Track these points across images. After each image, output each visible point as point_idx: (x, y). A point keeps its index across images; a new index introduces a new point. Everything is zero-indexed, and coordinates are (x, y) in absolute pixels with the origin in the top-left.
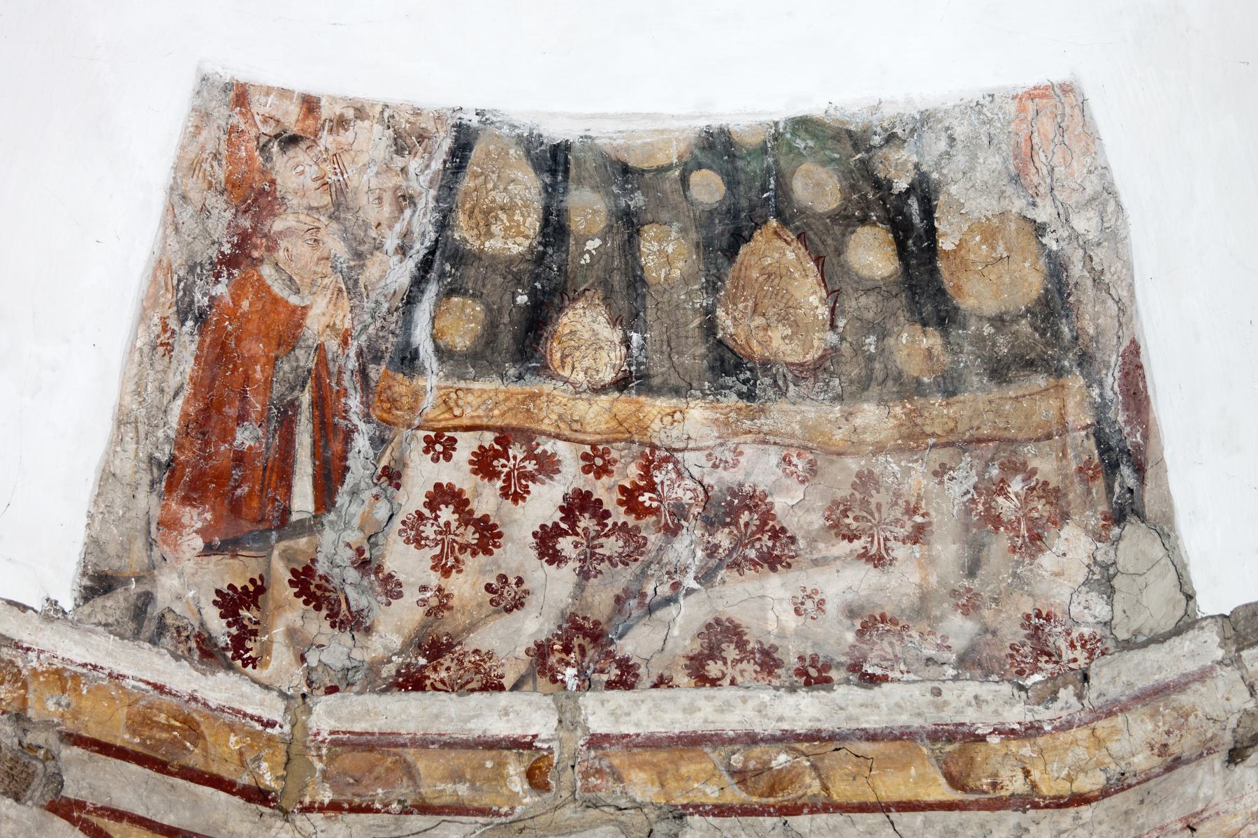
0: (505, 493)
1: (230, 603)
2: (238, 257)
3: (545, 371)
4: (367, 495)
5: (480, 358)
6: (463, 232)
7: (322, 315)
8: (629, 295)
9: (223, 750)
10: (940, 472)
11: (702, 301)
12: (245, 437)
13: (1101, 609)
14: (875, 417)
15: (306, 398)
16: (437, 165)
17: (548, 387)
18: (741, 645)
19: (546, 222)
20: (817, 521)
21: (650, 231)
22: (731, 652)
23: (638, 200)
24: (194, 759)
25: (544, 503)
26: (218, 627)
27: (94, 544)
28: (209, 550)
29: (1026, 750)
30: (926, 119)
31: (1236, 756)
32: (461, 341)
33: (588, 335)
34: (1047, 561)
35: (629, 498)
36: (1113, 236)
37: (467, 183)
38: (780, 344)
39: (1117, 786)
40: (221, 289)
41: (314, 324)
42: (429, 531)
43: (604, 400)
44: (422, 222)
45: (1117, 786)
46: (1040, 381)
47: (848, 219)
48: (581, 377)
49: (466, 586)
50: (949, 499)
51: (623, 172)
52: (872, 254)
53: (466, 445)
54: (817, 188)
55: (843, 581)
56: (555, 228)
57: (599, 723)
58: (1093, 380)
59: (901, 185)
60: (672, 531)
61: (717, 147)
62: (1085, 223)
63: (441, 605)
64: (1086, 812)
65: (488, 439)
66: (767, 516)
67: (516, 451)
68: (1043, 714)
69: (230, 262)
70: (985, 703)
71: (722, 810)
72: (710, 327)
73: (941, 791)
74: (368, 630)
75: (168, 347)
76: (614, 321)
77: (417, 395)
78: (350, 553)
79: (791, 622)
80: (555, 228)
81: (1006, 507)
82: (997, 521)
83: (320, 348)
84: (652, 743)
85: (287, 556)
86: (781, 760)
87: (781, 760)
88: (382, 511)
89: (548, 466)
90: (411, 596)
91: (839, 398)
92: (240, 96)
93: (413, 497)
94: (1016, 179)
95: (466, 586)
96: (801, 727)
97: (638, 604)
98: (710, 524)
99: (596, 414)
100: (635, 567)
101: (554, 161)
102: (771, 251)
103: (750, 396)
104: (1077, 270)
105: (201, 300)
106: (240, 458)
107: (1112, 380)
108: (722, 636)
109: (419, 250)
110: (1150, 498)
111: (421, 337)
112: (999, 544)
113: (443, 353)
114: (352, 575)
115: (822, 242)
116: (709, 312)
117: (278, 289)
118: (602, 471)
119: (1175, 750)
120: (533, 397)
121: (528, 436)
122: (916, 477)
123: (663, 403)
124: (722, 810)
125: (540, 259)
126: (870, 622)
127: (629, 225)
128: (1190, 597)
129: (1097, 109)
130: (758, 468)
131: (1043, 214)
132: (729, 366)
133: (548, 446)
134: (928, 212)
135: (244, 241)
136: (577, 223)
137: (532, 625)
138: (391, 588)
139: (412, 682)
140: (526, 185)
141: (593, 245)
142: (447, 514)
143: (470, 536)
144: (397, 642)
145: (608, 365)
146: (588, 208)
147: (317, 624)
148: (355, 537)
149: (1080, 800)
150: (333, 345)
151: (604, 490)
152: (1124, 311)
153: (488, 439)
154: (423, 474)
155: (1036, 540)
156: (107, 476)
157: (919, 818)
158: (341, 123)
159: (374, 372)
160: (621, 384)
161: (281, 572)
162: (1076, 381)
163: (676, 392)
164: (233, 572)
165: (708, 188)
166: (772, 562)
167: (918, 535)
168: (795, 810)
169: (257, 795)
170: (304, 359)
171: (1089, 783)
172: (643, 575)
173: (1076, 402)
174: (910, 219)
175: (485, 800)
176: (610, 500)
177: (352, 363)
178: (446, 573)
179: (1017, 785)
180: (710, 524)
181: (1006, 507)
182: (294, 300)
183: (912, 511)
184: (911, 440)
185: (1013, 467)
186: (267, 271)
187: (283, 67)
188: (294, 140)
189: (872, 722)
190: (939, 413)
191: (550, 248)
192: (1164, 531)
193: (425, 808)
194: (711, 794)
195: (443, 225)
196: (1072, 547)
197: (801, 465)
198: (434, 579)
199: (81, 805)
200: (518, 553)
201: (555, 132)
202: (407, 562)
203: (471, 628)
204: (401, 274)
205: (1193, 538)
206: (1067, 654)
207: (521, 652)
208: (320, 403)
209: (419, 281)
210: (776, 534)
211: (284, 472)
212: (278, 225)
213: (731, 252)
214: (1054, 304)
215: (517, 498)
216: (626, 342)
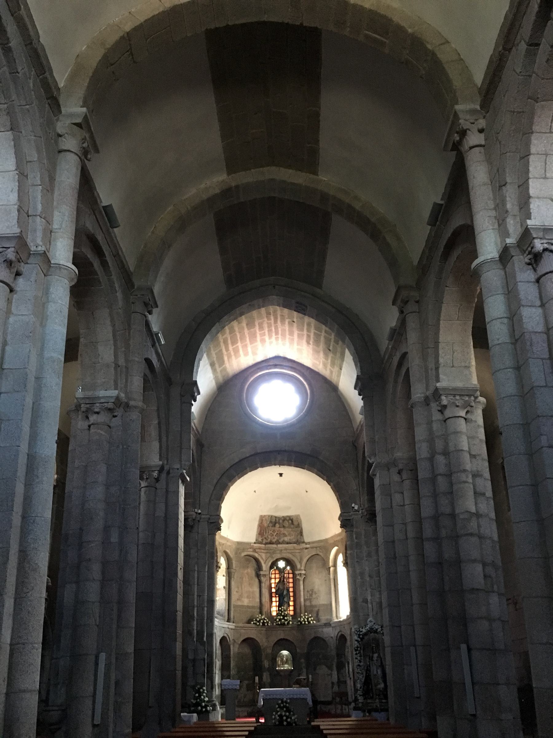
2: (262, 523)
5: (272, 526)
7: (266, 525)
8: (279, 523)
14: (290, 529)
25: (275, 534)
33: (277, 525)
36: (301, 521)
38: (286, 526)
51: (279, 518)
52: (290, 522)
54: (288, 519)
55: (289, 538)
61: (283, 517)
70: (295, 545)
97: (280, 539)
101: (276, 517)
102: (286, 521)
108: (284, 540)
115: (288, 521)
122: (292, 532)
130: (285, 532)
132: (284, 527)
146: (277, 519)
154: (270, 532)
173: (299, 529)
174: (292, 521)
187: (264, 514)
200: (274, 536)
202: (269, 537)
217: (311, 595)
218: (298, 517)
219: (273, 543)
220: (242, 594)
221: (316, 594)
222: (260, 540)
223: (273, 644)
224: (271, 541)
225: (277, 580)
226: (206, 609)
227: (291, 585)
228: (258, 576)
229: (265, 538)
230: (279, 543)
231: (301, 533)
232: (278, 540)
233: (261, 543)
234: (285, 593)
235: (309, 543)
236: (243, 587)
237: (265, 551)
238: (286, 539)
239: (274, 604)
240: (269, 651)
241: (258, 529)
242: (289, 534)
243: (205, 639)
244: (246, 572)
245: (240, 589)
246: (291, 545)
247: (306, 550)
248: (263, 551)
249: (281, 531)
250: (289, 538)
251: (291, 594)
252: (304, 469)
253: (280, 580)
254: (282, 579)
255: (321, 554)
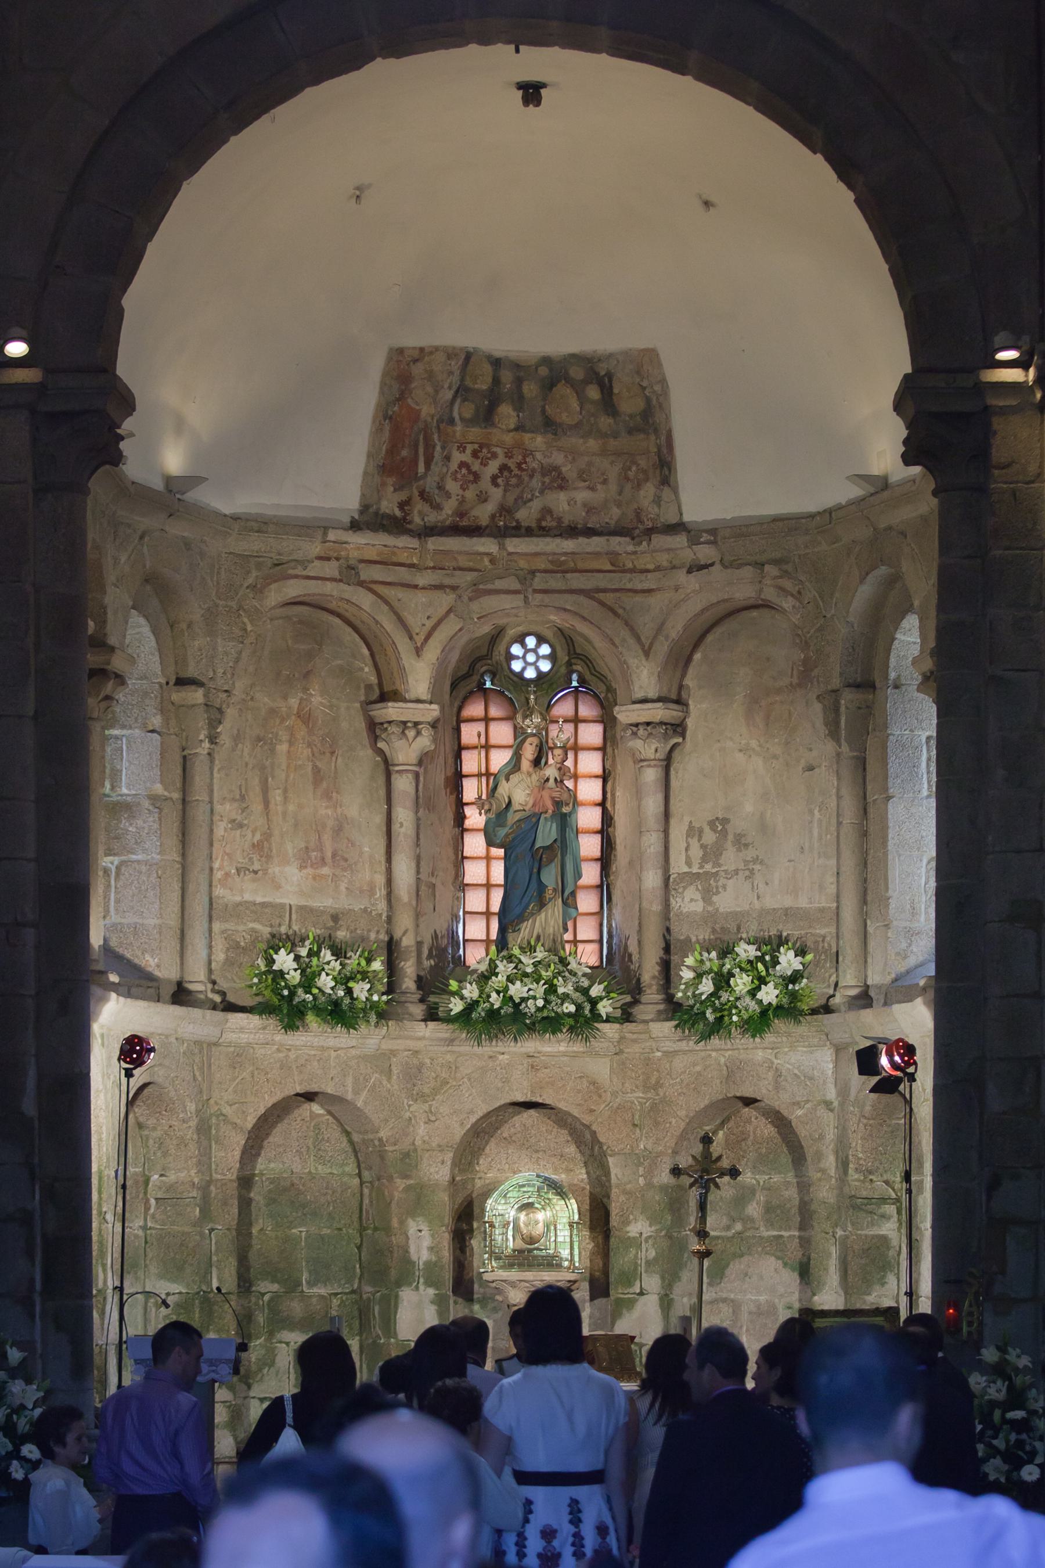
0: (481, 464)
1: (402, 505)
2: (401, 398)
3: (493, 425)
4: (440, 464)
6: (468, 382)
7: (427, 410)
8: (519, 401)
9: (403, 557)
10: (612, 463)
11: (541, 403)
12: (404, 453)
13: (656, 510)
14: (592, 444)
15: (421, 437)
16: (460, 363)
17: (495, 430)
18: (552, 516)
19: (493, 379)
20: (575, 475)
21: (525, 383)
22: (549, 518)
23: (522, 374)
24: (395, 559)
25: (493, 467)
26: (398, 513)
27: (363, 495)
28: (395, 490)
29: (633, 557)
30: (611, 355)
31: (689, 572)
32: (468, 415)
33: (507, 413)
34: (642, 493)
35: (519, 465)
36: (665, 392)
37: (470, 367)
38: (565, 418)
39: (658, 569)
40: (396, 409)
41: (423, 414)
42: (459, 476)
43: (511, 434)
44: (455, 379)
45: (658, 569)
46: (642, 436)
47: (586, 382)
48: (504, 427)
49: (470, 494)
50: (613, 473)
52: (593, 393)
53: (470, 448)
54: (577, 373)
55: (582, 496)
56: (496, 381)
57: (511, 549)
58: (658, 437)
59: (603, 373)
60: (531, 477)
61: (546, 361)
62: (657, 388)
63: (462, 501)
64: (649, 575)
65: (476, 446)
66: (560, 473)
67: (485, 450)
68: (638, 549)
69: (398, 400)
71: (546, 571)
72: (544, 411)
73: (609, 567)
74: (442, 509)
75: (381, 430)
76: (515, 410)
77: (454, 432)
78: (435, 484)
79: (566, 507)
80: (496, 381)
81: (631, 474)
82: (627, 479)
83: (425, 421)
84: (526, 554)
85: (417, 488)
86: (563, 558)
87: (563, 558)
88: (445, 470)
89: (494, 456)
90: (454, 498)
91: (582, 437)
92: (401, 351)
93: (454, 466)
94: (638, 373)
95: (470, 494)
96: (569, 551)
97: (522, 501)
98: (544, 475)
99: (509, 439)
100: (520, 488)
101: (497, 363)
102: (563, 390)
103: (555, 434)
104: (654, 402)
105: (390, 413)
106: (403, 459)
107: (663, 438)
108: (547, 511)
109: (455, 388)
110: (672, 479)
111: (456, 414)
112: (628, 486)
113: (462, 419)
114: (437, 491)
115: (579, 389)
116: (543, 407)
117: (413, 406)
118: (510, 457)
119: (674, 563)
120: (490, 433)
121: (488, 446)
123: (529, 435)
124: (546, 571)
125: (491, 390)
126: (590, 509)
127: (519, 381)
128: (681, 514)
129: (662, 356)
130: (558, 458)
131: (645, 384)
132: (550, 425)
133: (494, 449)
134: (610, 381)
135: (402, 393)
136: (503, 380)
137: (490, 507)
138: (448, 495)
139: (456, 530)
140: (488, 369)
141: (508, 386)
142: (464, 471)
143: (471, 478)
144: (450, 512)
145: (512, 423)
146: (507, 377)
147: (426, 508)
148: (437, 479)
149: (648, 571)
150: (429, 419)
151: (511, 464)
152: (668, 418)
153: (476, 446)
154: (457, 457)
155: (639, 486)
156: (366, 473)
157: (601, 575)
158: (431, 353)
159: (442, 426)
160: (516, 429)
161: (416, 493)
162: (653, 437)
163: (533, 432)
164: (403, 496)
165: (543, 371)
166: (561, 488)
167: (605, 482)
168: (566, 572)
169: (412, 566)
170: (421, 425)
171: (651, 567)
172: (522, 492)
175: (478, 567)
176: (513, 467)
177: (435, 424)
178: (464, 490)
179: (630, 565)
180: (544, 475)
181: (631, 474)
182: (418, 408)
183: (603, 474)
184: (604, 452)
185: (634, 462)
186: (409, 401)
187: (412, 341)
188: (417, 360)
189: (589, 549)
190: (612, 443)
191: (498, 388)
192: (675, 491)
193: (461, 569)
194: (543, 566)
195: (462, 380)
196: (648, 491)
197: (570, 458)
198: (461, 492)
199: (364, 582)
200: (485, 483)
201: (497, 354)
202: (452, 486)
203: (472, 508)
204: (449, 395)
205: (684, 497)
206: (647, 523)
207: (487, 516)
208: (426, 438)
209: (455, 397)
210: (563, 479)
211: (415, 462)
212: (413, 385)
213: (551, 389)
214: (647, 413)
215: (485, 465)
216: (518, 416)
217: (713, 854)
218: (645, 362)
219: (474, 531)
220: (267, 836)
221: (741, 842)
222: (389, 505)
223: (458, 1132)
224: (462, 515)
225: (500, 759)
226: (30, 935)
227: (590, 790)
228: (374, 729)
229: (422, 494)
230: (519, 531)
231: (664, 468)
232: (505, 510)
233: (396, 525)
234: (547, 834)
235: (713, 533)
236: (276, 796)
237: (422, 579)
238: (561, 503)
239: (475, 901)
240: (437, 1171)
241: (377, 430)
242: (582, 476)
243: (29, 1106)
244: (294, 702)
245: (257, 807)
246: (596, 543)
247: (691, 582)
248: (403, 574)
249: (527, 453)
250: (582, 496)
251: (590, 846)
252: (680, 69)
253: (517, 757)
254: (529, 752)
255: (787, 604)
